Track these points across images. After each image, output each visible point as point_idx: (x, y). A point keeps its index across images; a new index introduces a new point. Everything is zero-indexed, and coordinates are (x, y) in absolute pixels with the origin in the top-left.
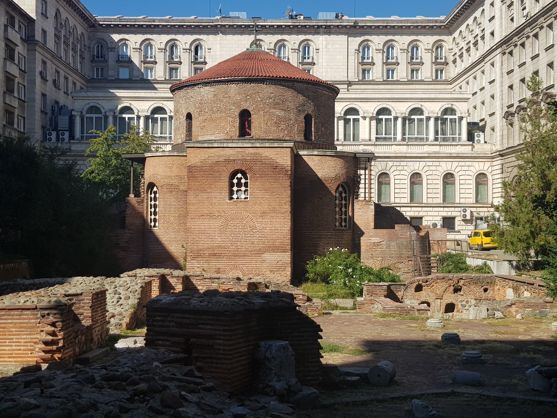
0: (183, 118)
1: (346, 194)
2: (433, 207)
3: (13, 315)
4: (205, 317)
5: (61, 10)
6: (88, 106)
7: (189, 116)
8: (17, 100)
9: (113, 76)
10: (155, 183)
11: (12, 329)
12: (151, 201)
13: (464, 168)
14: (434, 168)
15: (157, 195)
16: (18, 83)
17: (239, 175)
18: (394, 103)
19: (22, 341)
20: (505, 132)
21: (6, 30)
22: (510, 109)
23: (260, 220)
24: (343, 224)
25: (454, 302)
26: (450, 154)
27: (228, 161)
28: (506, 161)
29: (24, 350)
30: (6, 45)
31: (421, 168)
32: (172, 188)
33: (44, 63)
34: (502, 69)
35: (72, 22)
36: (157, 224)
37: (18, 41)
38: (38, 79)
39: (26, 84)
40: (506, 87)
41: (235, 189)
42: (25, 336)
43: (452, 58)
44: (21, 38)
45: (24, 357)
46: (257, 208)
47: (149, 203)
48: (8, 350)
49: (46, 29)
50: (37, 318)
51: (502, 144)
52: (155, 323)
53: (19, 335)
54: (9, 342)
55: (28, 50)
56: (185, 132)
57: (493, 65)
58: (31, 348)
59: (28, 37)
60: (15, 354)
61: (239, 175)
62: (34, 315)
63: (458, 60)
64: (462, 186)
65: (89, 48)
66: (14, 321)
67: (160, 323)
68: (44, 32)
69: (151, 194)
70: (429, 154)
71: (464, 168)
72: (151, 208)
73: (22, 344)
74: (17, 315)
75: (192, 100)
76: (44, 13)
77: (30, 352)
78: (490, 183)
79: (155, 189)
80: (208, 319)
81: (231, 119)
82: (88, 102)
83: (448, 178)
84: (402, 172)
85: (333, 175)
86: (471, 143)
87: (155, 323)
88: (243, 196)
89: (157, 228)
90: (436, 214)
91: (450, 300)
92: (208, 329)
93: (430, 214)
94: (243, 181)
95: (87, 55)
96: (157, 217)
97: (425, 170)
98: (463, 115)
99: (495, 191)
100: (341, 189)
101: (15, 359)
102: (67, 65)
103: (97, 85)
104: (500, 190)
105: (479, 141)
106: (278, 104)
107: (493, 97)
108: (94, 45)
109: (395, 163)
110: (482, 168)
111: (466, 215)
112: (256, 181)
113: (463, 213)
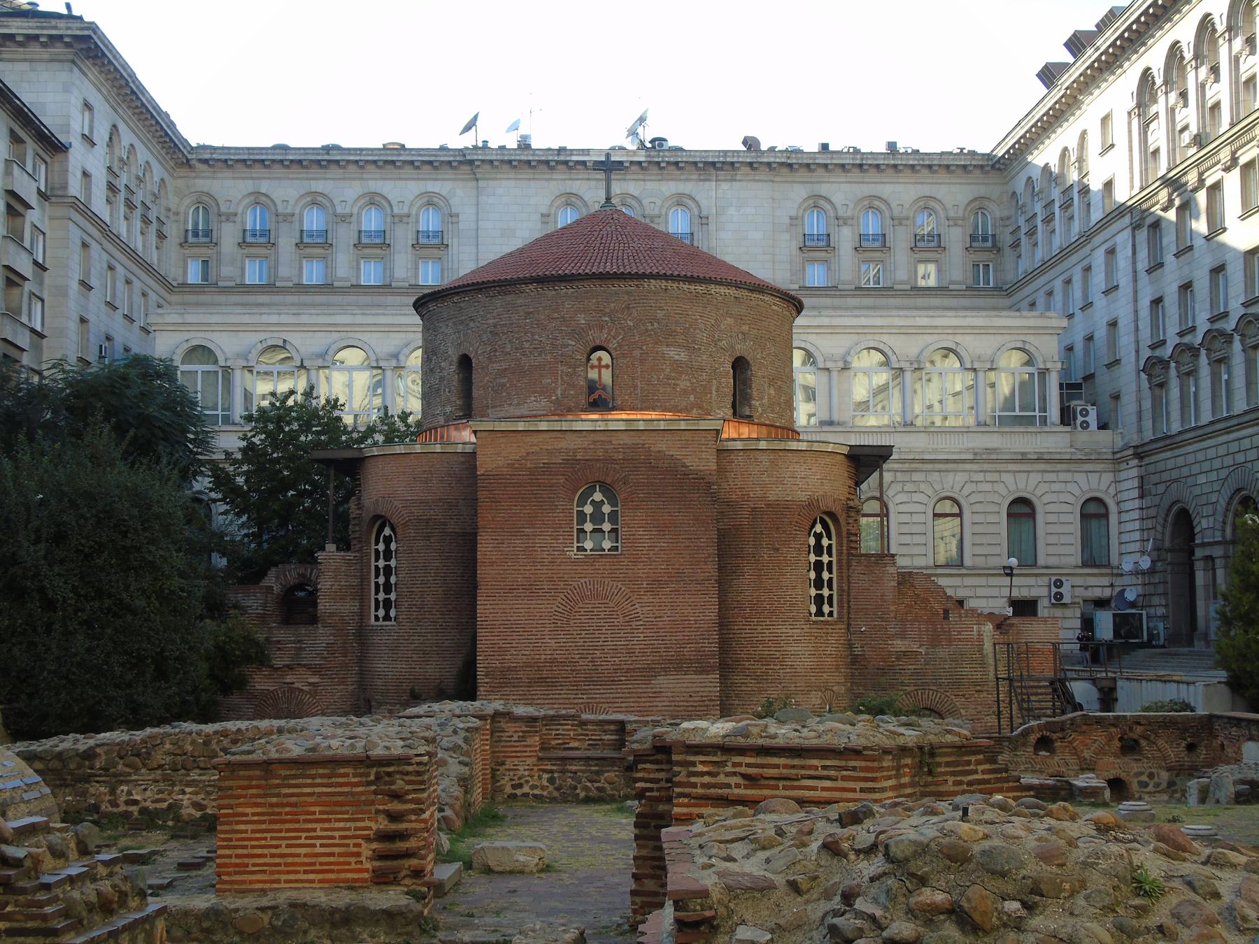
0: (450, 369)
1: (830, 539)
2: (987, 575)
3: (313, 777)
4: (815, 762)
5: (122, 127)
6: (186, 346)
7: (465, 363)
8: (28, 333)
9: (231, 279)
10: (388, 515)
11: (313, 809)
12: (377, 560)
13: (1055, 487)
14: (988, 487)
15: (393, 546)
16: (32, 294)
17: (598, 496)
18: (893, 337)
19: (337, 834)
20: (1147, 404)
21: (8, 172)
22: (1158, 353)
23: (645, 599)
24: (826, 609)
25: (1123, 776)
26: (1023, 454)
28: (1151, 468)
29: (340, 855)
30: (9, 206)
31: (957, 489)
33: (85, 245)
34: (1134, 262)
35: (143, 154)
36: (393, 613)
37: (33, 199)
38: (75, 286)
39: (45, 297)
40: (1145, 303)
41: (588, 527)
42: (341, 825)
43: (1009, 240)
44: (39, 191)
45: (339, 871)
47: (373, 563)
48: (305, 855)
49: (91, 169)
50: (369, 783)
51: (1140, 431)
52: (693, 780)
53: (329, 820)
54: (306, 838)
55: (51, 218)
57: (1111, 252)
58: (356, 850)
59: (52, 189)
60: (321, 864)
61: (598, 496)
62: (361, 775)
63: (1024, 240)
64: (1051, 529)
65: (177, 214)
66: (318, 790)
67: (706, 779)
68: (86, 174)
69: (377, 544)
70: (975, 454)
71: (1055, 487)
72: (377, 576)
73: (337, 841)
74: (322, 776)
75: (472, 324)
76: (86, 132)
77: (353, 860)
78: (1113, 518)
79: (387, 531)
80: (824, 768)
81: (565, 369)
82: (187, 336)
83: (1022, 509)
84: (916, 497)
85: (803, 496)
86: (1068, 429)
87: (693, 780)
88: (607, 544)
89: (393, 623)
90: (995, 592)
91: (1114, 772)
92: (824, 789)
93: (980, 592)
94: (606, 509)
95: (173, 232)
96: (393, 596)
97: (965, 492)
98: (1049, 365)
99: (1125, 538)
100: (818, 528)
101: (320, 876)
102: (132, 254)
103: (192, 298)
104: (1137, 536)
105: (1085, 425)
107: (1113, 324)
108: (188, 207)
109: (900, 476)
110: (1094, 486)
111: (1061, 595)
113: (1054, 590)
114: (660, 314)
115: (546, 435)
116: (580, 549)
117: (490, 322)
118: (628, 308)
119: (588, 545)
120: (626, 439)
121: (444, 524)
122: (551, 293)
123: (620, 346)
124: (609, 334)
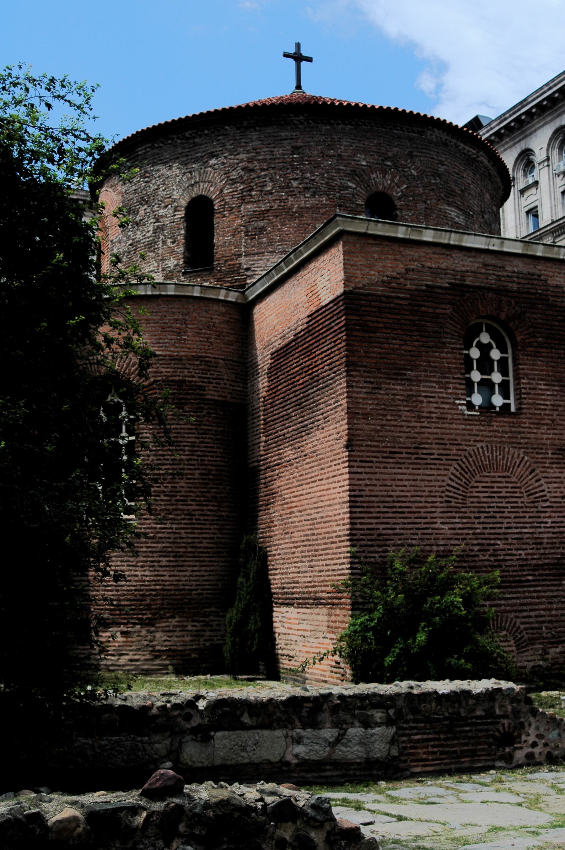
23: (553, 472)
27: (459, 289)
32: (183, 393)
46: (545, 435)
56: (181, 249)
61: (485, 338)
75: (213, 161)
94: (495, 354)
106: (451, 193)
112: (536, 355)
114: (442, 169)
115: (429, 250)
116: (470, 406)
117: (242, 156)
118: (411, 155)
119: (477, 399)
120: (520, 266)
121: (201, 388)
122: (324, 128)
123: (404, 195)
124: (392, 180)
